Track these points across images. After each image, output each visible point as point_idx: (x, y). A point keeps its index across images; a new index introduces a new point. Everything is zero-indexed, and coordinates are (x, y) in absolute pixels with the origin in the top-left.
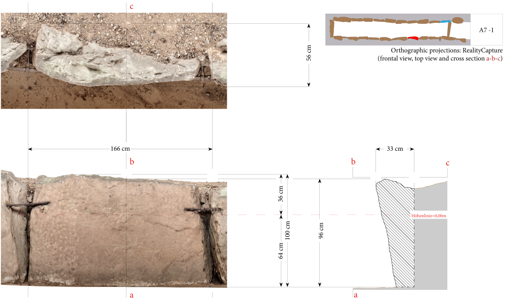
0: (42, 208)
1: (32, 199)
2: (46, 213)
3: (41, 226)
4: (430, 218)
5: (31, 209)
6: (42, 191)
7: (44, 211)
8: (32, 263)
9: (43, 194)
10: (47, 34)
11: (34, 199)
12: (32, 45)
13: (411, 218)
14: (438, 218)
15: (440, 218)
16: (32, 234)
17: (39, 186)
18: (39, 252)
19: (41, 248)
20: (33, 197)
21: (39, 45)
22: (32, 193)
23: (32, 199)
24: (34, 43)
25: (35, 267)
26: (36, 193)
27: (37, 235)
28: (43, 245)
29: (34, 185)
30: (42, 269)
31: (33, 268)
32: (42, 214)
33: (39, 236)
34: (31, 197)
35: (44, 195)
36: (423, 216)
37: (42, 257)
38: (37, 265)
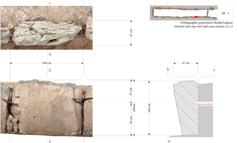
0: (89, 101)
1: (85, 96)
2: (91, 103)
3: (89, 109)
4: (205, 105)
5: (84, 101)
6: (90, 93)
7: (90, 102)
8: (85, 126)
9: (90, 94)
10: (91, 21)
11: (86, 96)
12: (84, 26)
13: (196, 105)
14: (209, 105)
15: (210, 105)
16: (84, 113)
17: (88, 90)
18: (88, 121)
19: (89, 119)
20: (85, 95)
21: (88, 26)
22: (85, 93)
23: (85, 96)
24: (85, 26)
25: (86, 128)
26: (86, 94)
27: (87, 113)
28: (90, 118)
29: (85, 90)
30: (89, 129)
31: (85, 128)
32: (89, 103)
33: (88, 114)
34: (84, 96)
35: (91, 94)
36: (201, 104)
37: (89, 123)
38: (87, 127)
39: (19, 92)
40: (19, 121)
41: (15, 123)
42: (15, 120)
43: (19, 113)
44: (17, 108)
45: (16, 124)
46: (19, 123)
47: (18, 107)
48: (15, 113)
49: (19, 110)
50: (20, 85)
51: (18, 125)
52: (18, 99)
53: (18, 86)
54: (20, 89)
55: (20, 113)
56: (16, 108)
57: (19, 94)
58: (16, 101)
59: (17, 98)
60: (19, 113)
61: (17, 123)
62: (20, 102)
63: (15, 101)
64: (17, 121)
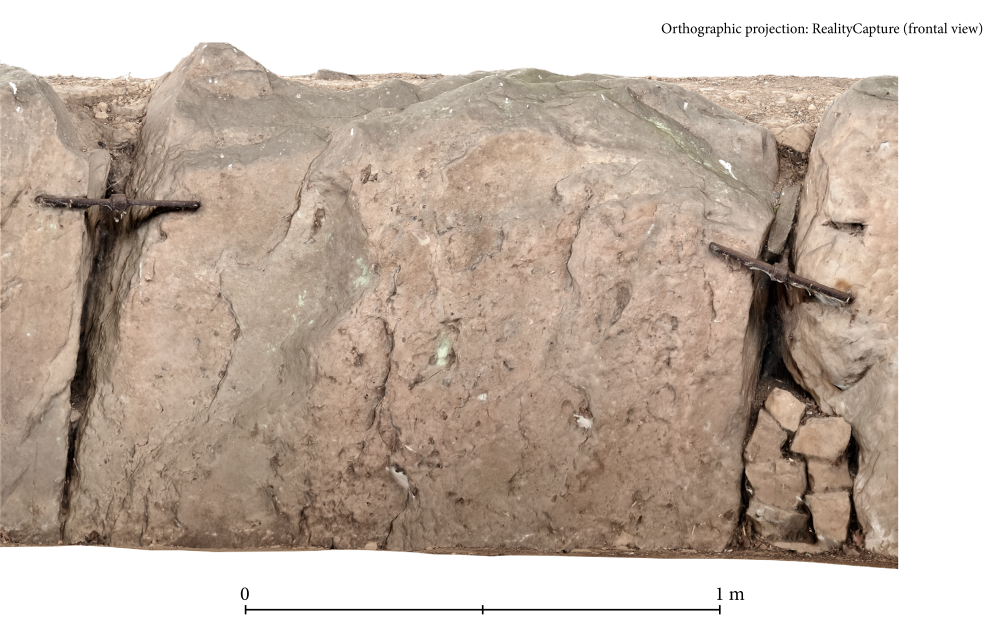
39: (860, 180)
40: (863, 442)
41: (828, 460)
42: (826, 439)
43: (862, 375)
44: (844, 322)
45: (833, 476)
46: (865, 459)
47: (853, 317)
48: (825, 373)
49: (863, 347)
50: (869, 121)
51: (847, 482)
52: (855, 240)
53: (856, 123)
54: (869, 156)
55: (868, 368)
56: (834, 324)
57: (862, 200)
58: (833, 264)
59: (845, 239)
60: (858, 369)
61: (837, 463)
62: (867, 273)
63: (825, 261)
64: (844, 442)
